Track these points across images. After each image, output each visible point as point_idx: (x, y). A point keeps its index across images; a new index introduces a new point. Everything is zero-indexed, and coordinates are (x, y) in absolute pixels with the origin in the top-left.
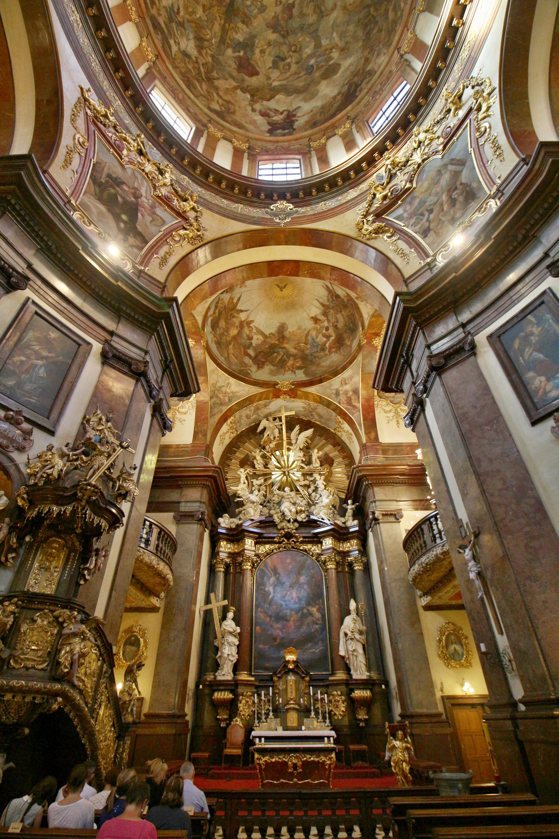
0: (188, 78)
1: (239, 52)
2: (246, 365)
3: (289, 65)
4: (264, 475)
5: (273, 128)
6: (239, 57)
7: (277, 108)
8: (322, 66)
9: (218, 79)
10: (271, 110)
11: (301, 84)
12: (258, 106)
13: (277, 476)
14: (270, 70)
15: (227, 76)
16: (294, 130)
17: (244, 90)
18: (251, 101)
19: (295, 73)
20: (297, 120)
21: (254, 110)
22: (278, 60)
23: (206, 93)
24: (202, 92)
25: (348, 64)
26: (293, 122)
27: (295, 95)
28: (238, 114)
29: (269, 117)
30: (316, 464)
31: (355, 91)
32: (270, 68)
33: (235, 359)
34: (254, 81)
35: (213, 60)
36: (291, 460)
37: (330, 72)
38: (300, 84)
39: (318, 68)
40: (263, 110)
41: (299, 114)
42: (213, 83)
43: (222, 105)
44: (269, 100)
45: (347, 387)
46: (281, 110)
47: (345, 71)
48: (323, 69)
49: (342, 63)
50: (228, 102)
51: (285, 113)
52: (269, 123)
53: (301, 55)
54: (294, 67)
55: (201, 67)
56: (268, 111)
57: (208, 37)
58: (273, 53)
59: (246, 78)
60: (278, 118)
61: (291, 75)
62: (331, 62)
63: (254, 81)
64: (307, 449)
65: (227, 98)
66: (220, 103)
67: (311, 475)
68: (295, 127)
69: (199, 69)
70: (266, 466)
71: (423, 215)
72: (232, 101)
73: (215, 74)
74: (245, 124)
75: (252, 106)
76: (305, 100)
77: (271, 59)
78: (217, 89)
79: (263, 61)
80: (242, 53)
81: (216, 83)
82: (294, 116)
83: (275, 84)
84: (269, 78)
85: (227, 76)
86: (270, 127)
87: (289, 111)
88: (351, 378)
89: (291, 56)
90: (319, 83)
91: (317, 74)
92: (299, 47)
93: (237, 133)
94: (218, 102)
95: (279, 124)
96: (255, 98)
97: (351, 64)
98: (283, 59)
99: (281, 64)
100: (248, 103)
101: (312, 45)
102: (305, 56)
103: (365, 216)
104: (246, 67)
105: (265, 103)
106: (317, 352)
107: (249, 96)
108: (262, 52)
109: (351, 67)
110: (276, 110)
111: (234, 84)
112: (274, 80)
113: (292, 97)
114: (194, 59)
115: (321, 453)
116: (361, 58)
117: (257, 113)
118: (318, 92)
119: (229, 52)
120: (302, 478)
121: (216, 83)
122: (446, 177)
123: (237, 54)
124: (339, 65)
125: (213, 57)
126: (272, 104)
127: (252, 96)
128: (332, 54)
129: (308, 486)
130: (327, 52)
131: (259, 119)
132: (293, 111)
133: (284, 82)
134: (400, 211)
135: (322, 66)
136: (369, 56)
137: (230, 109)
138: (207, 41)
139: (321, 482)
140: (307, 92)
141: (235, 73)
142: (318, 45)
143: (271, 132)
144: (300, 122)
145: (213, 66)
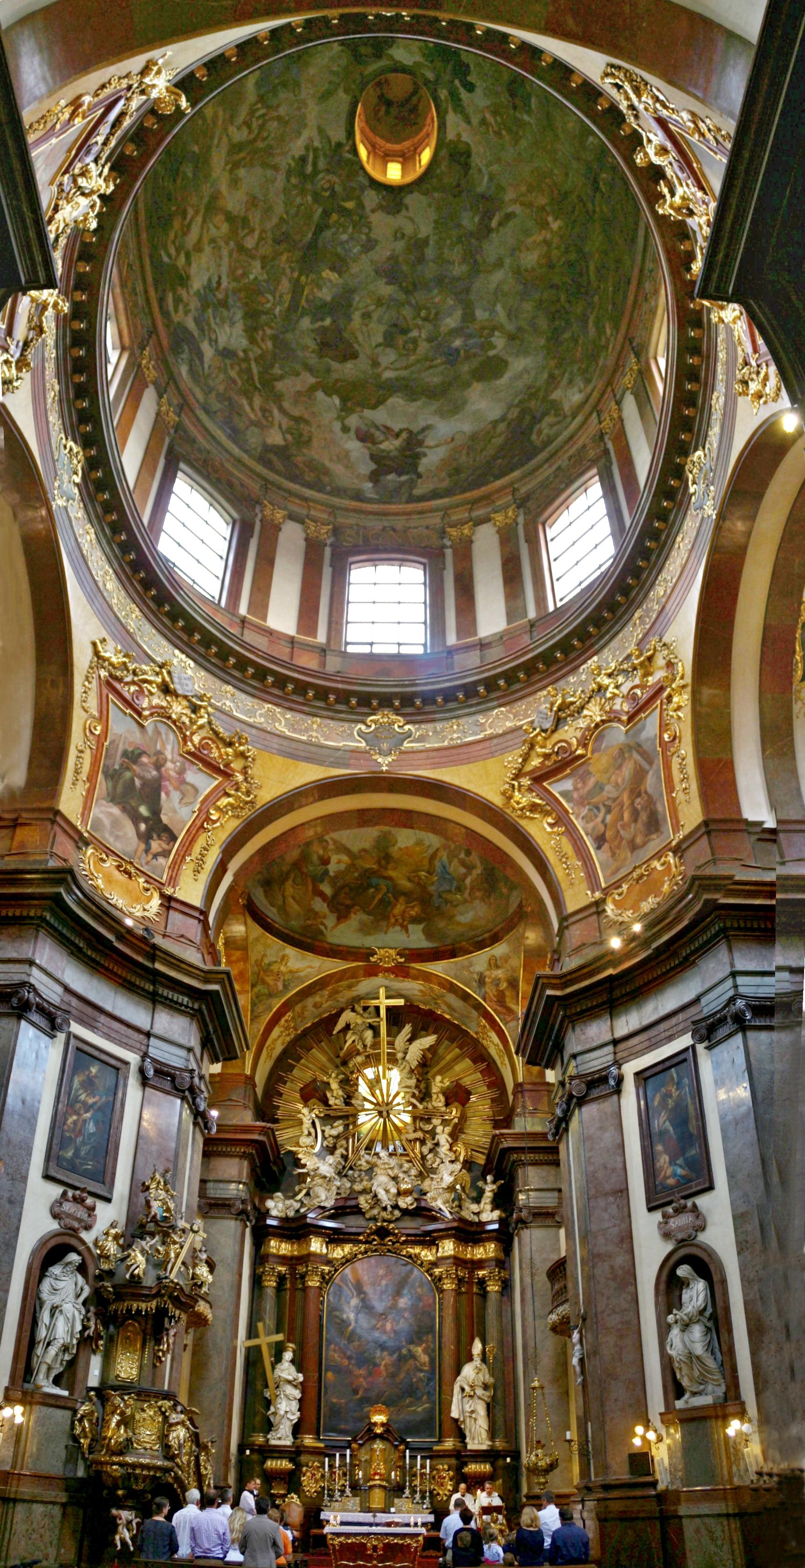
0: (230, 399)
1: (322, 320)
2: (316, 915)
3: (415, 341)
4: (345, 1117)
5: (382, 464)
6: (323, 331)
7: (389, 424)
8: (475, 355)
9: (281, 378)
10: (377, 428)
11: (437, 380)
12: (353, 421)
13: (367, 1121)
14: (380, 349)
15: (298, 367)
16: (419, 476)
17: (328, 393)
18: (342, 410)
19: (426, 359)
20: (425, 455)
21: (345, 429)
22: (395, 333)
23: (259, 414)
24: (252, 416)
25: (522, 366)
26: (418, 456)
27: (423, 399)
28: (315, 443)
29: (374, 443)
30: (438, 1102)
31: (531, 428)
32: (379, 345)
33: (296, 907)
34: (348, 370)
35: (275, 346)
36: (394, 1089)
37: (491, 369)
38: (434, 378)
39: (467, 358)
40: (364, 428)
41: (429, 442)
42: (273, 387)
43: (289, 431)
44: (374, 407)
45: (499, 973)
46: (396, 429)
47: (519, 376)
48: (475, 363)
49: (510, 360)
50: (298, 420)
51: (404, 435)
52: (373, 457)
53: (436, 326)
54: (423, 347)
55: (253, 365)
56: (373, 430)
57: (269, 305)
58: (386, 317)
59: (335, 365)
60: (390, 445)
61: (418, 361)
62: (492, 353)
63: (348, 370)
64: (424, 1069)
65: (296, 412)
66: (284, 427)
67: (428, 1121)
68: (421, 469)
69: (249, 371)
70: (347, 1103)
71: (598, 809)
72: (306, 416)
73: (277, 370)
74: (327, 463)
75: (340, 418)
76: (443, 414)
77: (382, 329)
78: (278, 398)
79: (367, 333)
80: (328, 322)
81: (279, 386)
82: (420, 443)
83: (388, 375)
84: (375, 364)
85: (298, 367)
86: (373, 466)
87: (410, 432)
88: (506, 959)
89: (419, 328)
90: (468, 385)
91: (465, 368)
92: (433, 311)
93: (314, 501)
94: (280, 427)
95: (392, 459)
96: (349, 404)
97: (526, 370)
98: (404, 331)
99: (400, 340)
100: (334, 414)
101: (459, 313)
102: (443, 329)
103: (516, 777)
104: (335, 345)
105: (367, 413)
106: (450, 891)
107: (337, 401)
108: (367, 316)
109: (526, 376)
110: (388, 428)
111: (312, 380)
112: (387, 368)
113: (419, 403)
114: (241, 354)
115: (447, 1083)
116: (544, 368)
117: (352, 434)
118: (465, 403)
119: (305, 323)
120: (411, 1128)
121: (279, 386)
122: (627, 770)
123: (320, 323)
124: (506, 363)
125: (274, 338)
126: (380, 416)
127: (344, 400)
128: (493, 339)
129: (423, 1142)
130: (486, 332)
131: (353, 446)
132: (419, 433)
133: (404, 373)
134: (568, 785)
135: (475, 355)
136: (557, 372)
137: (301, 435)
138: (266, 313)
139: (443, 1138)
140: (445, 396)
141: (313, 360)
142: (468, 316)
143: (374, 477)
144: (432, 459)
145: (275, 355)
